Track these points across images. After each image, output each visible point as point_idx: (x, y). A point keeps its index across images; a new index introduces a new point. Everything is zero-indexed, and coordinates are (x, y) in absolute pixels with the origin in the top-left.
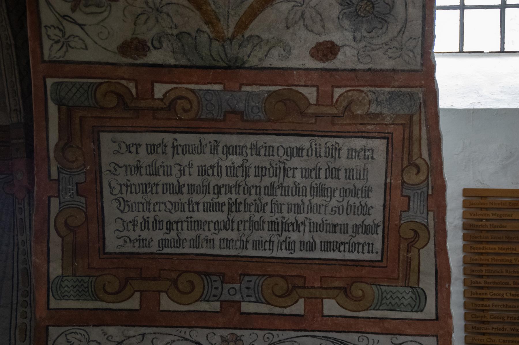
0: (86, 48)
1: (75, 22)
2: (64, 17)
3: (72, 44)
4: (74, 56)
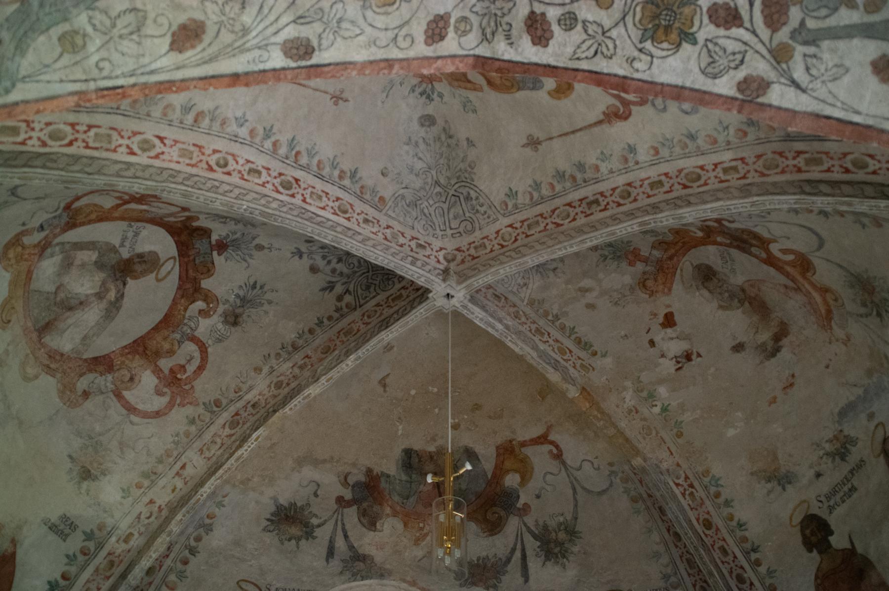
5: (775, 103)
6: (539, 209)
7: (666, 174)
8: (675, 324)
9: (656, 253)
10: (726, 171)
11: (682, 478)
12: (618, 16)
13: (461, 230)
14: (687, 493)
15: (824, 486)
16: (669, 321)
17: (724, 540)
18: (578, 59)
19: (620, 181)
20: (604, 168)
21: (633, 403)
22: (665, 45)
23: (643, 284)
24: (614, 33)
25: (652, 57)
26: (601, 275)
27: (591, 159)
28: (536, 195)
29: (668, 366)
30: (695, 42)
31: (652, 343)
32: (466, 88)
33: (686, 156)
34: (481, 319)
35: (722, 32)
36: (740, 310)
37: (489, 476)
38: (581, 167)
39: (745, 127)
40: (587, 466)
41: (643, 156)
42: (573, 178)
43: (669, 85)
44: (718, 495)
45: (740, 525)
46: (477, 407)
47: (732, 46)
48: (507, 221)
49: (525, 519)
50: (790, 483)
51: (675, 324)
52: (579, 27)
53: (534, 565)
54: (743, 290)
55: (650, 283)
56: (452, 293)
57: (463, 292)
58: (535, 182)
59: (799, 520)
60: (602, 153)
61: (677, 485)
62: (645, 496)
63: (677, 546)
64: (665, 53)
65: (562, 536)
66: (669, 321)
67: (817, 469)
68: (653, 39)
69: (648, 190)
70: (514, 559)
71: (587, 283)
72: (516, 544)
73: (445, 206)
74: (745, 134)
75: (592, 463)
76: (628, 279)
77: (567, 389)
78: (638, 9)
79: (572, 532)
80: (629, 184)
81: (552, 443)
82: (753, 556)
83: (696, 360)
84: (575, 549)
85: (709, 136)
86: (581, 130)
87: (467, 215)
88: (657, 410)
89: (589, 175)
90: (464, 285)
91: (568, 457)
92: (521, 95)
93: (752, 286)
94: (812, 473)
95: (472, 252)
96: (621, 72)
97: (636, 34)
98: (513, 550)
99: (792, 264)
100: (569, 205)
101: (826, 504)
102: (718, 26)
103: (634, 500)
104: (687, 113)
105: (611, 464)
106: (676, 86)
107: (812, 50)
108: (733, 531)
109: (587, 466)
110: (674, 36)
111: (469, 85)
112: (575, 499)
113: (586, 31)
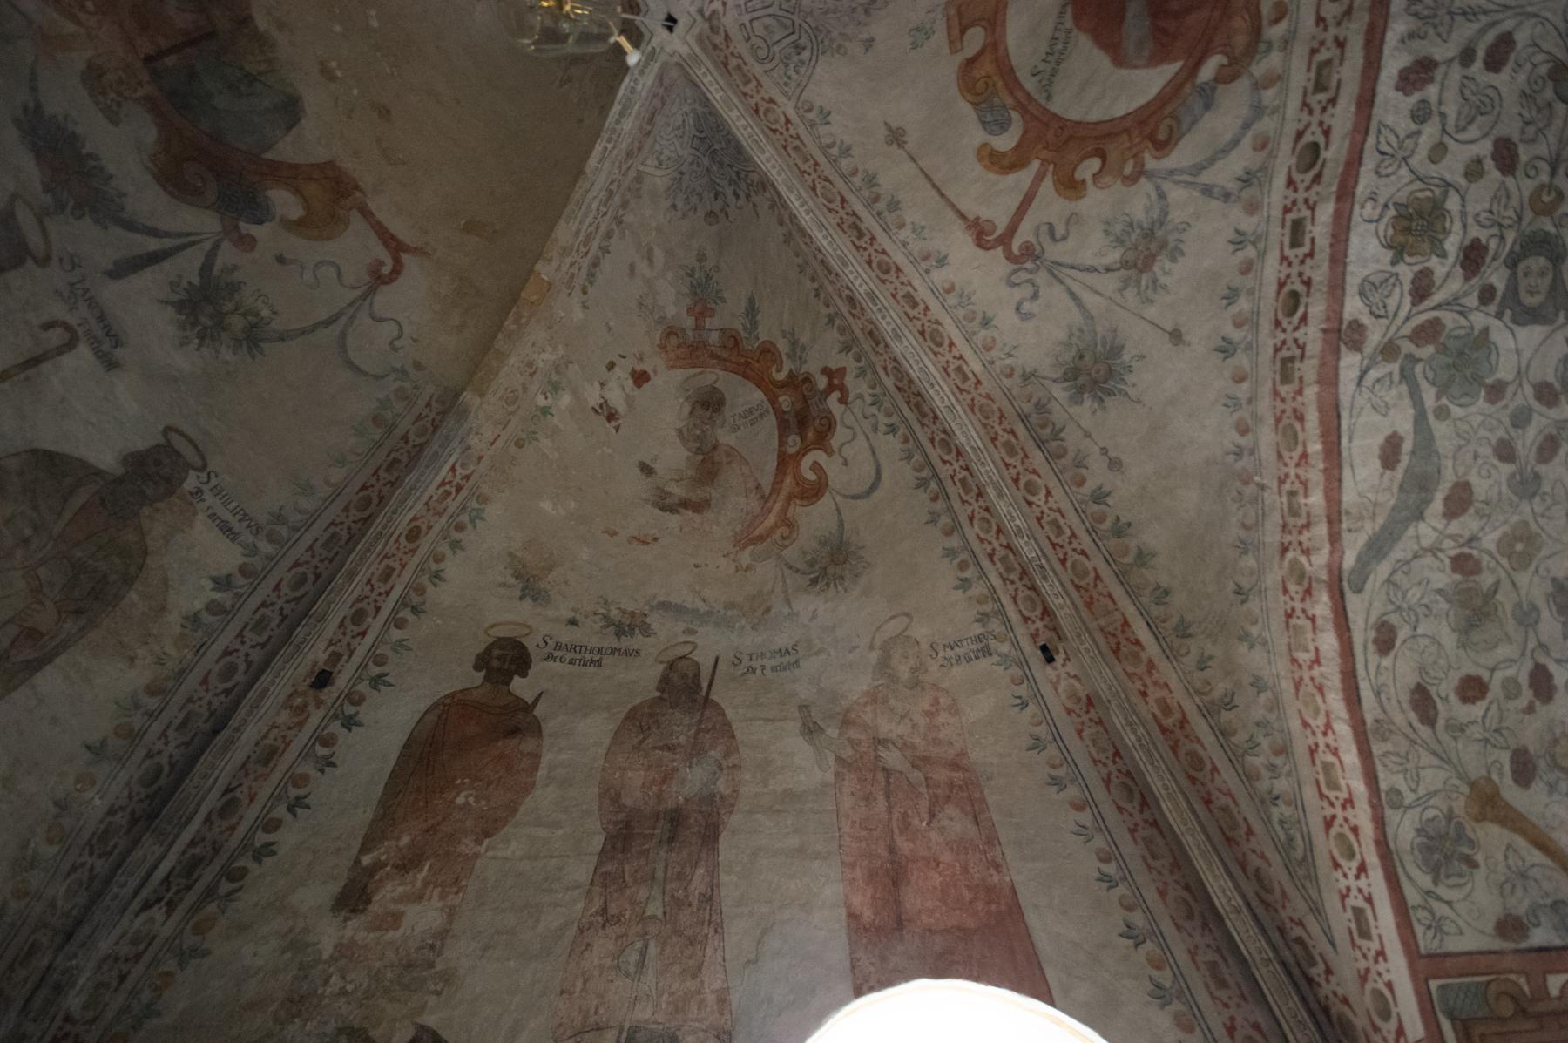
0: (1461, 933)
1: (1439, 899)
2: (1428, 893)
3: (1446, 928)
4: (1454, 944)
5: (1342, 363)
6: (821, 159)
7: (927, 308)
8: (639, 386)
9: (714, 337)
10: (959, 369)
11: (465, 472)
12: (1422, 171)
13: (754, 40)
14: (447, 487)
15: (567, 635)
16: (640, 378)
17: (403, 566)
18: (1379, 132)
19: (898, 257)
20: (905, 234)
21: (541, 365)
22: (1390, 232)
23: (670, 332)
24: (1404, 171)
25: (1377, 221)
26: (670, 275)
27: (910, 216)
28: (834, 151)
29: (593, 396)
30: (1393, 263)
31: (611, 366)
32: (949, 28)
33: (957, 323)
34: (633, 90)
35: (1407, 287)
36: (687, 453)
37: (268, 156)
38: (894, 205)
39: (1018, 372)
40: (389, 330)
41: (939, 276)
42: (876, 199)
43: (1346, 250)
44: (460, 528)
45: (437, 576)
46: (384, 112)
47: (1392, 303)
48: (792, 114)
49: (226, 245)
50: (535, 600)
51: (639, 386)
52: (1414, 127)
53: (149, 281)
54: (715, 447)
55: (673, 340)
56: (680, 28)
57: (684, 50)
58: (849, 148)
59: (501, 635)
60: (923, 228)
61: (453, 469)
62: (399, 432)
63: (346, 509)
64: (1381, 234)
65: (237, 323)
66: (640, 378)
67: (578, 617)
68: (1399, 217)
69: (901, 293)
70: (139, 238)
71: (659, 255)
72: (167, 235)
73: (774, 10)
74: (1010, 376)
75: (399, 337)
76: (671, 311)
77: (550, 260)
78: (1428, 193)
79: (254, 337)
80: (898, 270)
81: (398, 263)
82: (406, 613)
83: (610, 427)
84: (227, 354)
85: (994, 340)
86: (942, 195)
87: (776, 48)
88: (541, 401)
89: (890, 218)
90: (697, 50)
91: (384, 299)
92: (965, 108)
93: (728, 455)
94: (571, 614)
95: (733, 62)
96: (1360, 189)
97: (1402, 197)
98: (153, 232)
99: (799, 479)
100: (843, 200)
101: (547, 650)
102: (1413, 282)
103: (377, 420)
104: (1017, 309)
105: (417, 365)
106: (1346, 256)
107: (1396, 377)
108: (422, 570)
109: (389, 330)
110: (1401, 239)
111: (956, 32)
112: (315, 327)
113: (1408, 136)
